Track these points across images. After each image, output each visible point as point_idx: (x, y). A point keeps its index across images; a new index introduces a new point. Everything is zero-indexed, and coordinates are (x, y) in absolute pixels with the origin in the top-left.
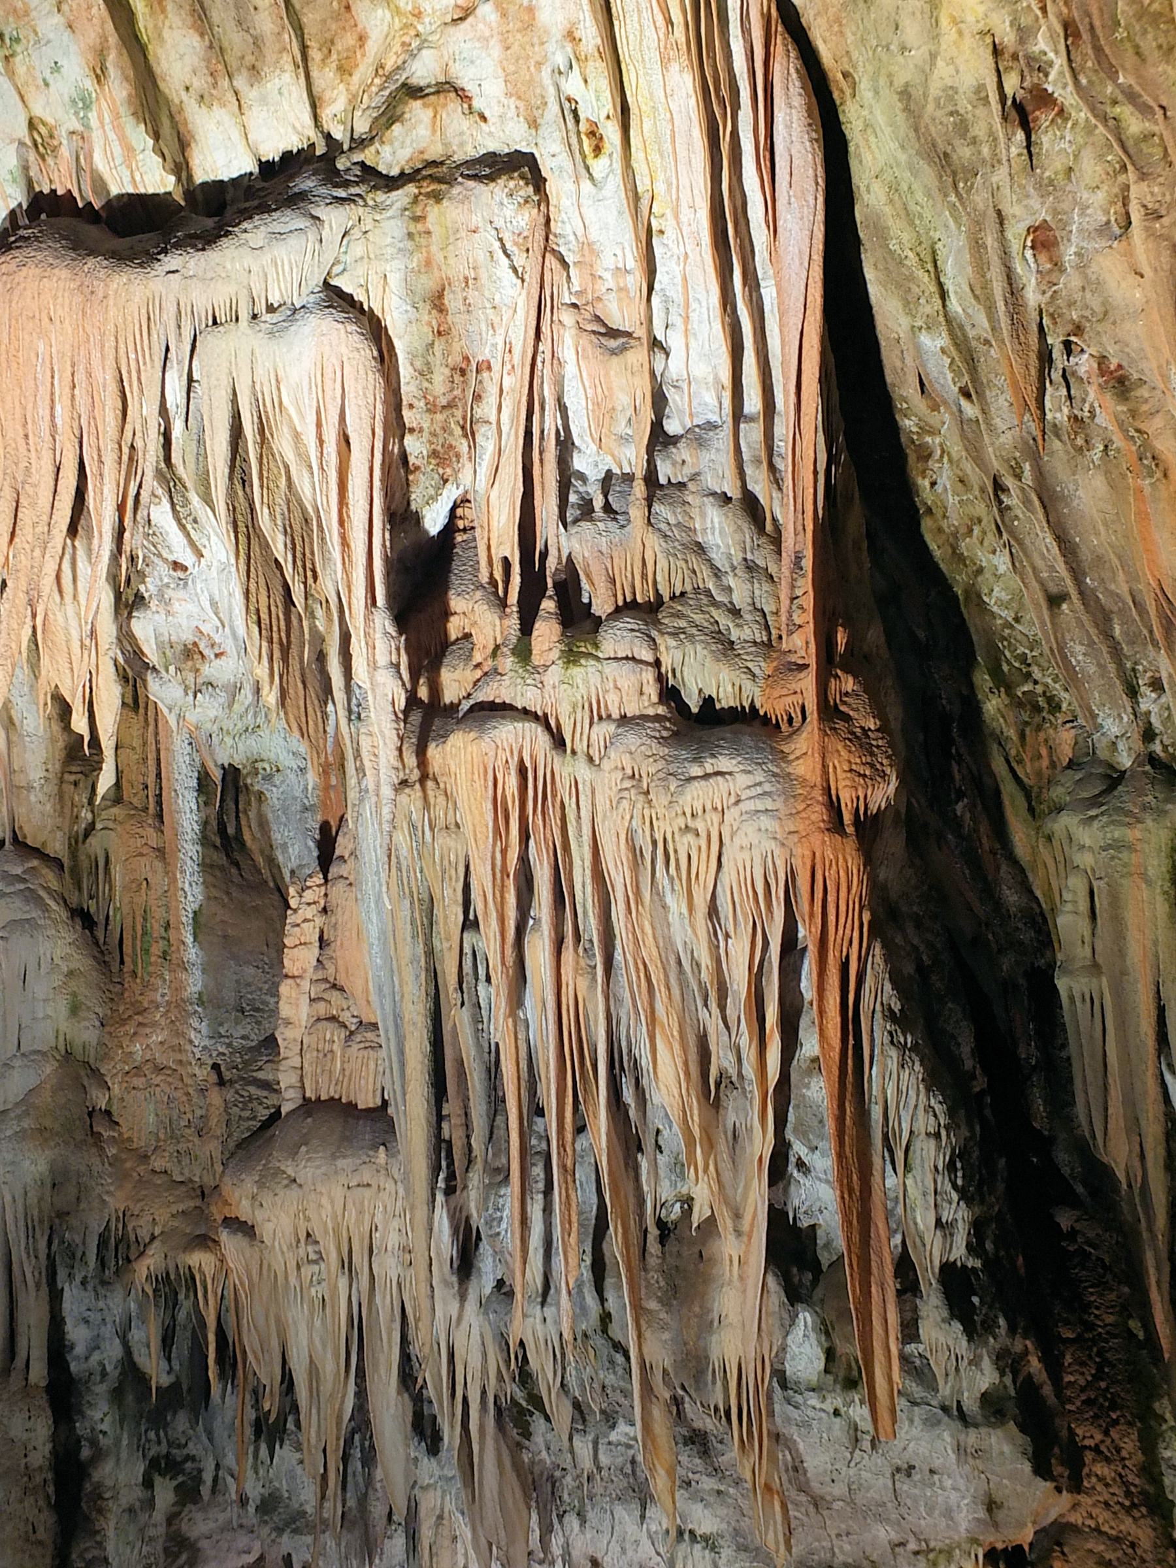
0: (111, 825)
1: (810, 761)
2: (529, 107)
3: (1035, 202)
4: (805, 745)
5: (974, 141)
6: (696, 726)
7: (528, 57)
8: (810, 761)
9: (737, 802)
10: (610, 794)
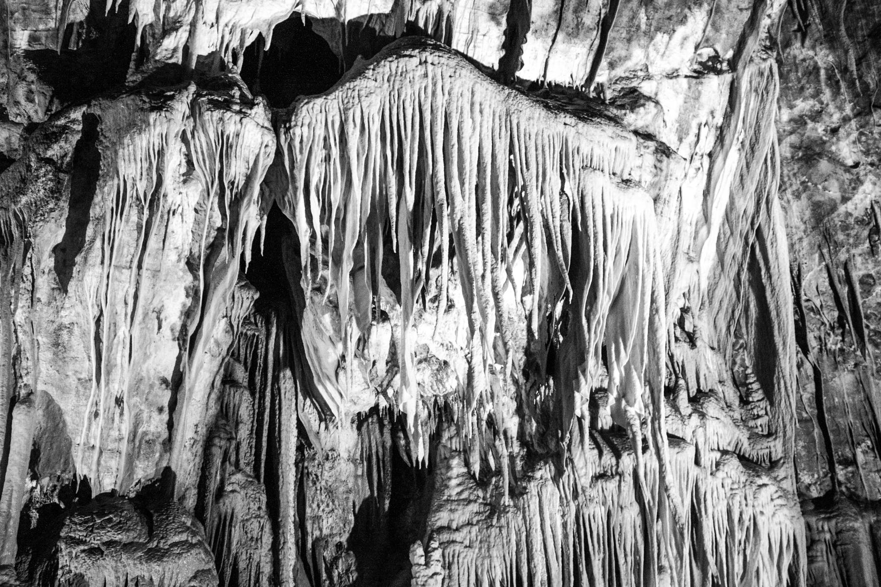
0: (238, 489)
1: (789, 480)
2: (681, 131)
3: (870, 265)
5: (848, 235)
7: (690, 111)
8: (789, 480)
9: (772, 500)
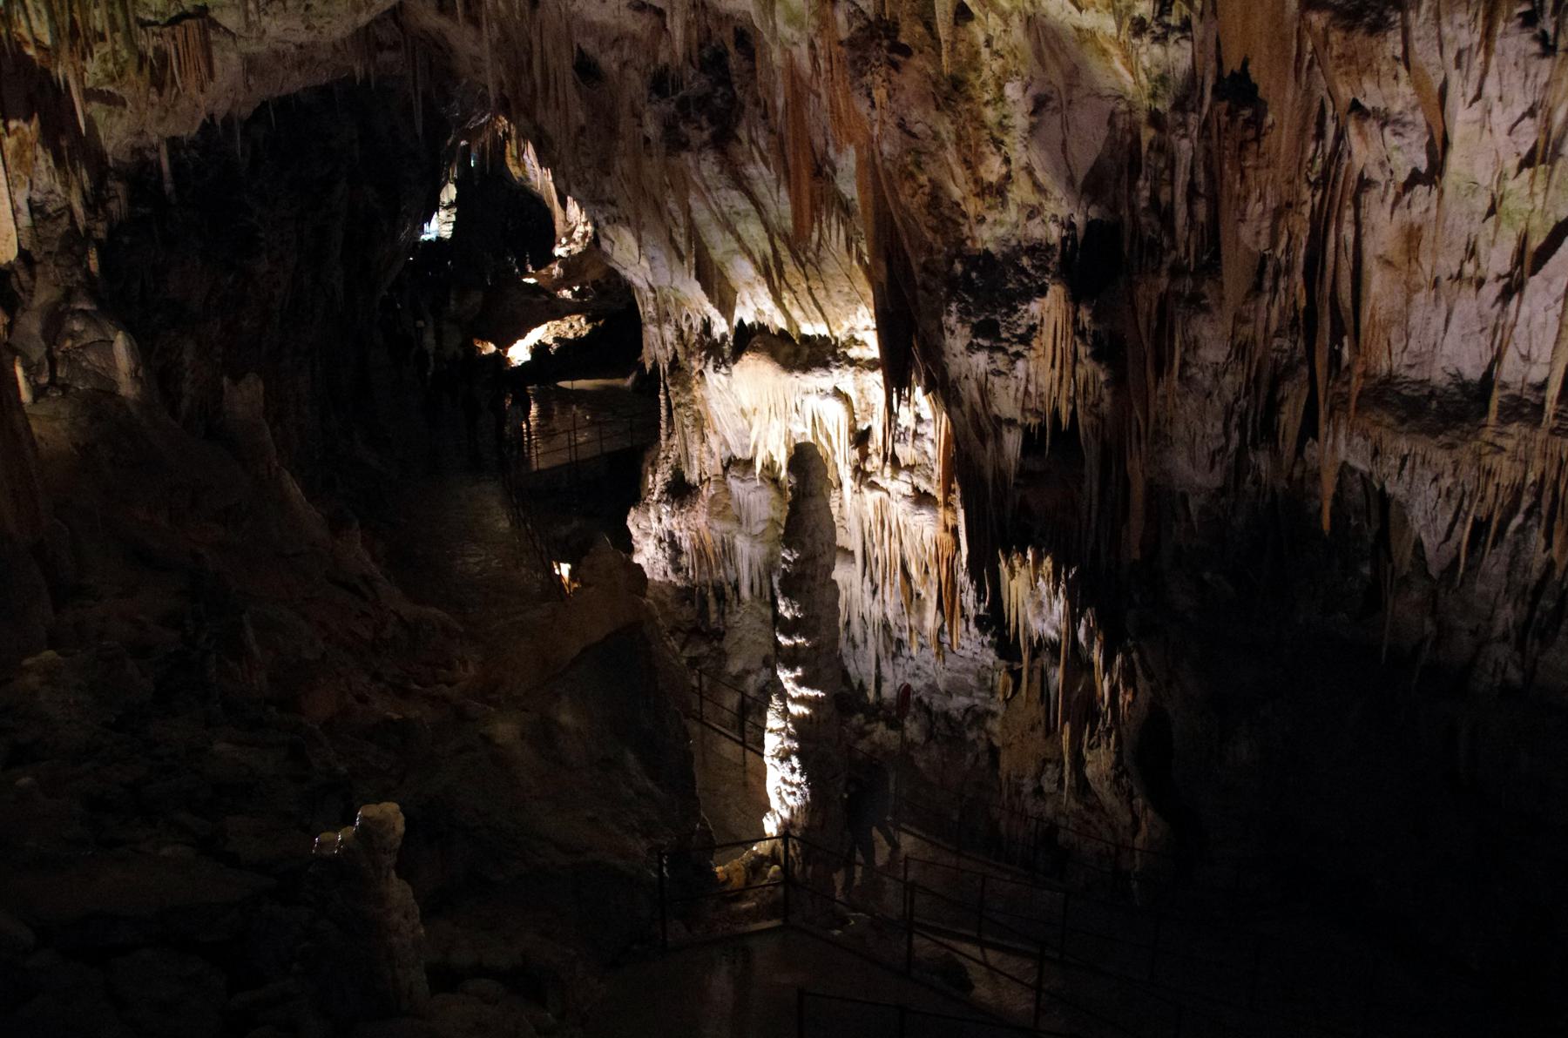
4: (941, 510)
6: (921, 499)
10: (900, 510)
